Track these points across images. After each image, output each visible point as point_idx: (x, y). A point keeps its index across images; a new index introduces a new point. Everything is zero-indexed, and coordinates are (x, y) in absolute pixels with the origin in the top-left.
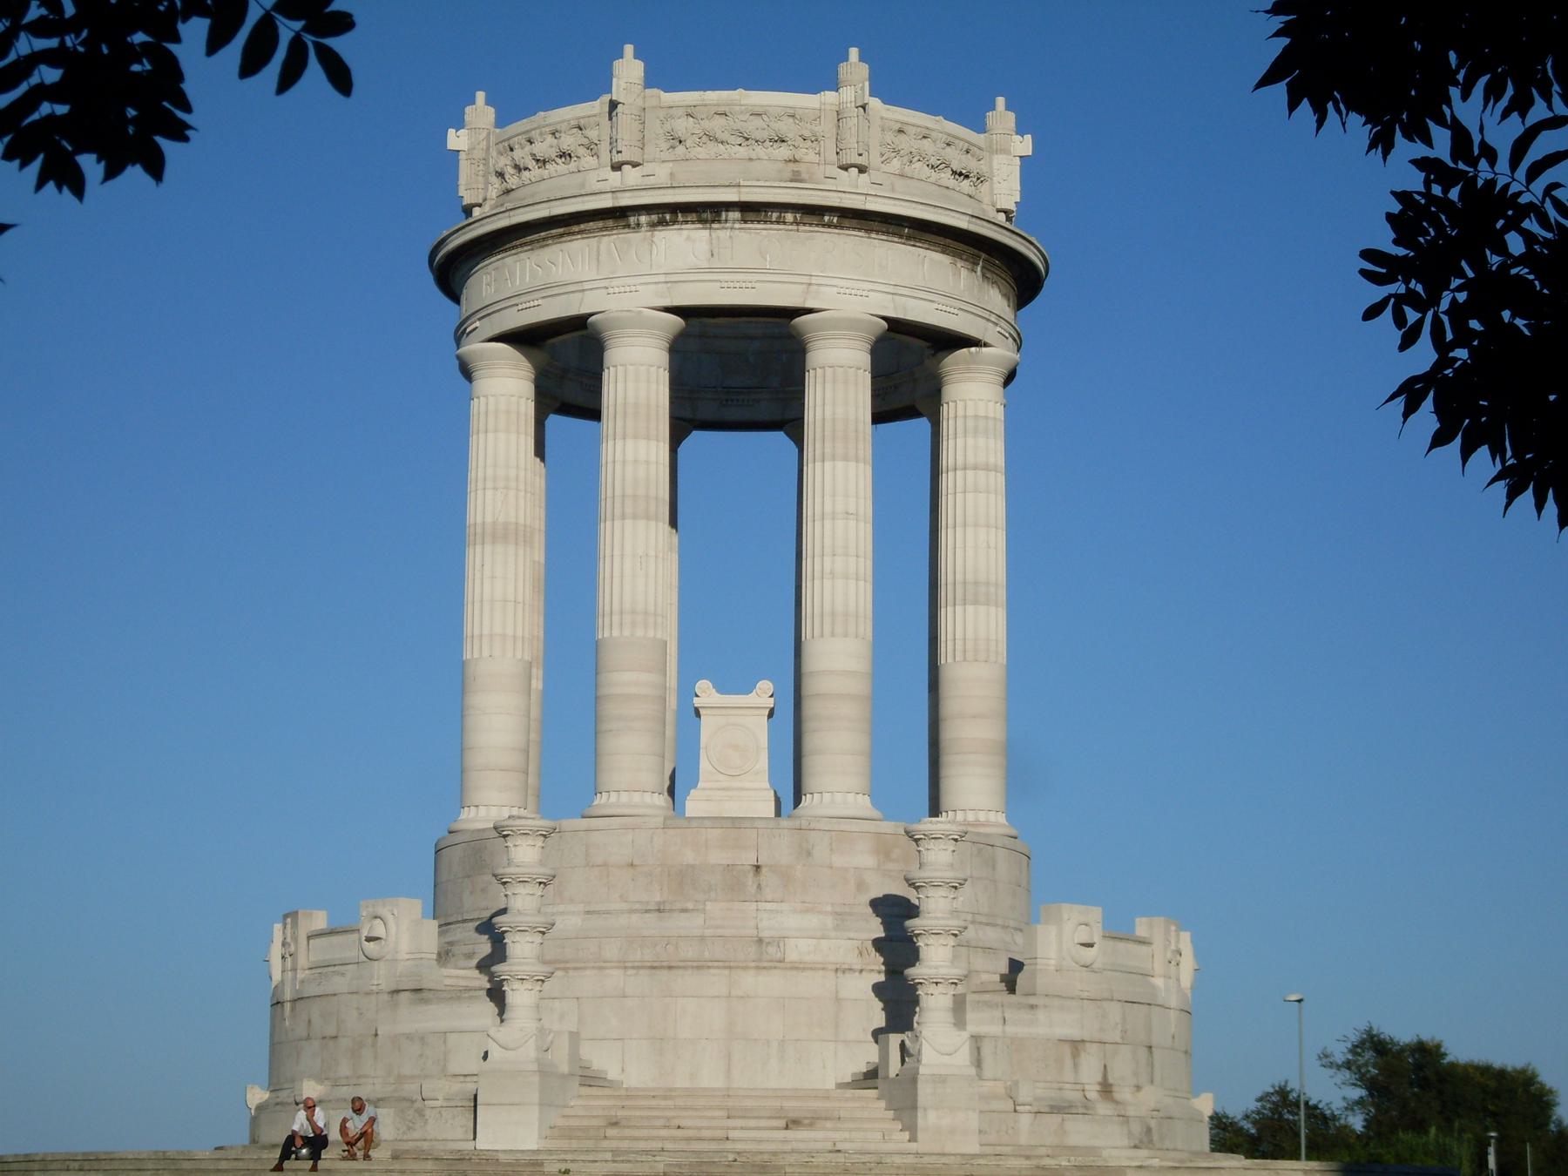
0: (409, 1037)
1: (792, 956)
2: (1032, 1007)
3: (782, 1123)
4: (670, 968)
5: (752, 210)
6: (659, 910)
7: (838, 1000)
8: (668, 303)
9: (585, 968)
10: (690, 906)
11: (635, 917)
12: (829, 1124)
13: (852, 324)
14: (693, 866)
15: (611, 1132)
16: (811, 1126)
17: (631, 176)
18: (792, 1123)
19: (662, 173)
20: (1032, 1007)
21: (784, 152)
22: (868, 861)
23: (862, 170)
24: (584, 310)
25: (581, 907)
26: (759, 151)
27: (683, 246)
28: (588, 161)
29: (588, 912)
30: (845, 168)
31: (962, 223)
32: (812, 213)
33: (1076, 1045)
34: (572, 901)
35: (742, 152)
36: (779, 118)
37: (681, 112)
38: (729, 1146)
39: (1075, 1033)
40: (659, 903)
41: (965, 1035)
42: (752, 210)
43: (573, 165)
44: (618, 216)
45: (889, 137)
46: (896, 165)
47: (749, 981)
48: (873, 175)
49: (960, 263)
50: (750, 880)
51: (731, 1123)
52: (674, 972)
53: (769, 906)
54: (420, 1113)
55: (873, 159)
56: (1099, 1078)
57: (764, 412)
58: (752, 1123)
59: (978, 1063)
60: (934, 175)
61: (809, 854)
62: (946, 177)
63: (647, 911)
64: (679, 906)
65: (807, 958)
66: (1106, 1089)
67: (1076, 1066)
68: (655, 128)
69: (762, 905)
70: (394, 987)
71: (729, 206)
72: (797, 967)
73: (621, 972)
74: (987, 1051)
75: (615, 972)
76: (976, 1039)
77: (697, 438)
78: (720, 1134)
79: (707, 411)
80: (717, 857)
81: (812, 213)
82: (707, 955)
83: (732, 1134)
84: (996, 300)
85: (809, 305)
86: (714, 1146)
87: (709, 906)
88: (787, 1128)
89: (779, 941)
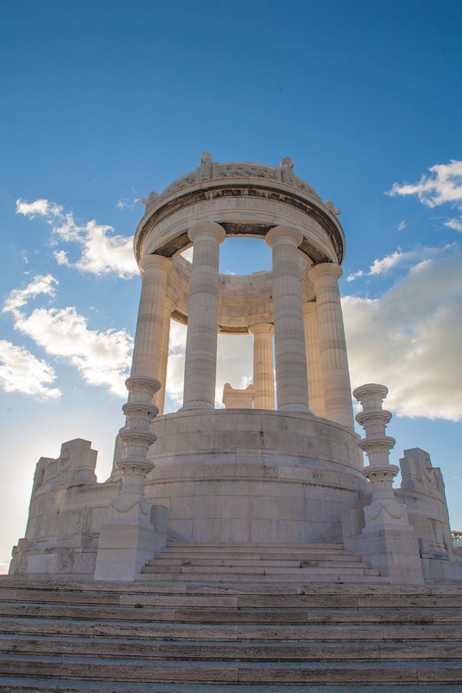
0: (73, 512)
1: (281, 476)
2: (415, 499)
3: (298, 564)
4: (218, 480)
6: (213, 453)
7: (305, 499)
8: (220, 220)
9: (174, 482)
10: (228, 450)
11: (200, 456)
12: (327, 565)
14: (230, 432)
15: (185, 569)
16: (316, 566)
18: (305, 564)
22: (313, 434)
25: (173, 454)
29: (177, 456)
34: (169, 451)
37: (225, 168)
38: (268, 579)
40: (212, 449)
50: (258, 438)
52: (221, 483)
53: (268, 451)
56: (443, 541)
58: (279, 564)
63: (207, 454)
64: (224, 451)
65: (288, 477)
69: (265, 451)
70: (70, 486)
72: (284, 481)
73: (192, 484)
75: (189, 484)
78: (260, 571)
80: (241, 427)
82: (238, 474)
85: (275, 223)
87: (238, 450)
88: (301, 567)
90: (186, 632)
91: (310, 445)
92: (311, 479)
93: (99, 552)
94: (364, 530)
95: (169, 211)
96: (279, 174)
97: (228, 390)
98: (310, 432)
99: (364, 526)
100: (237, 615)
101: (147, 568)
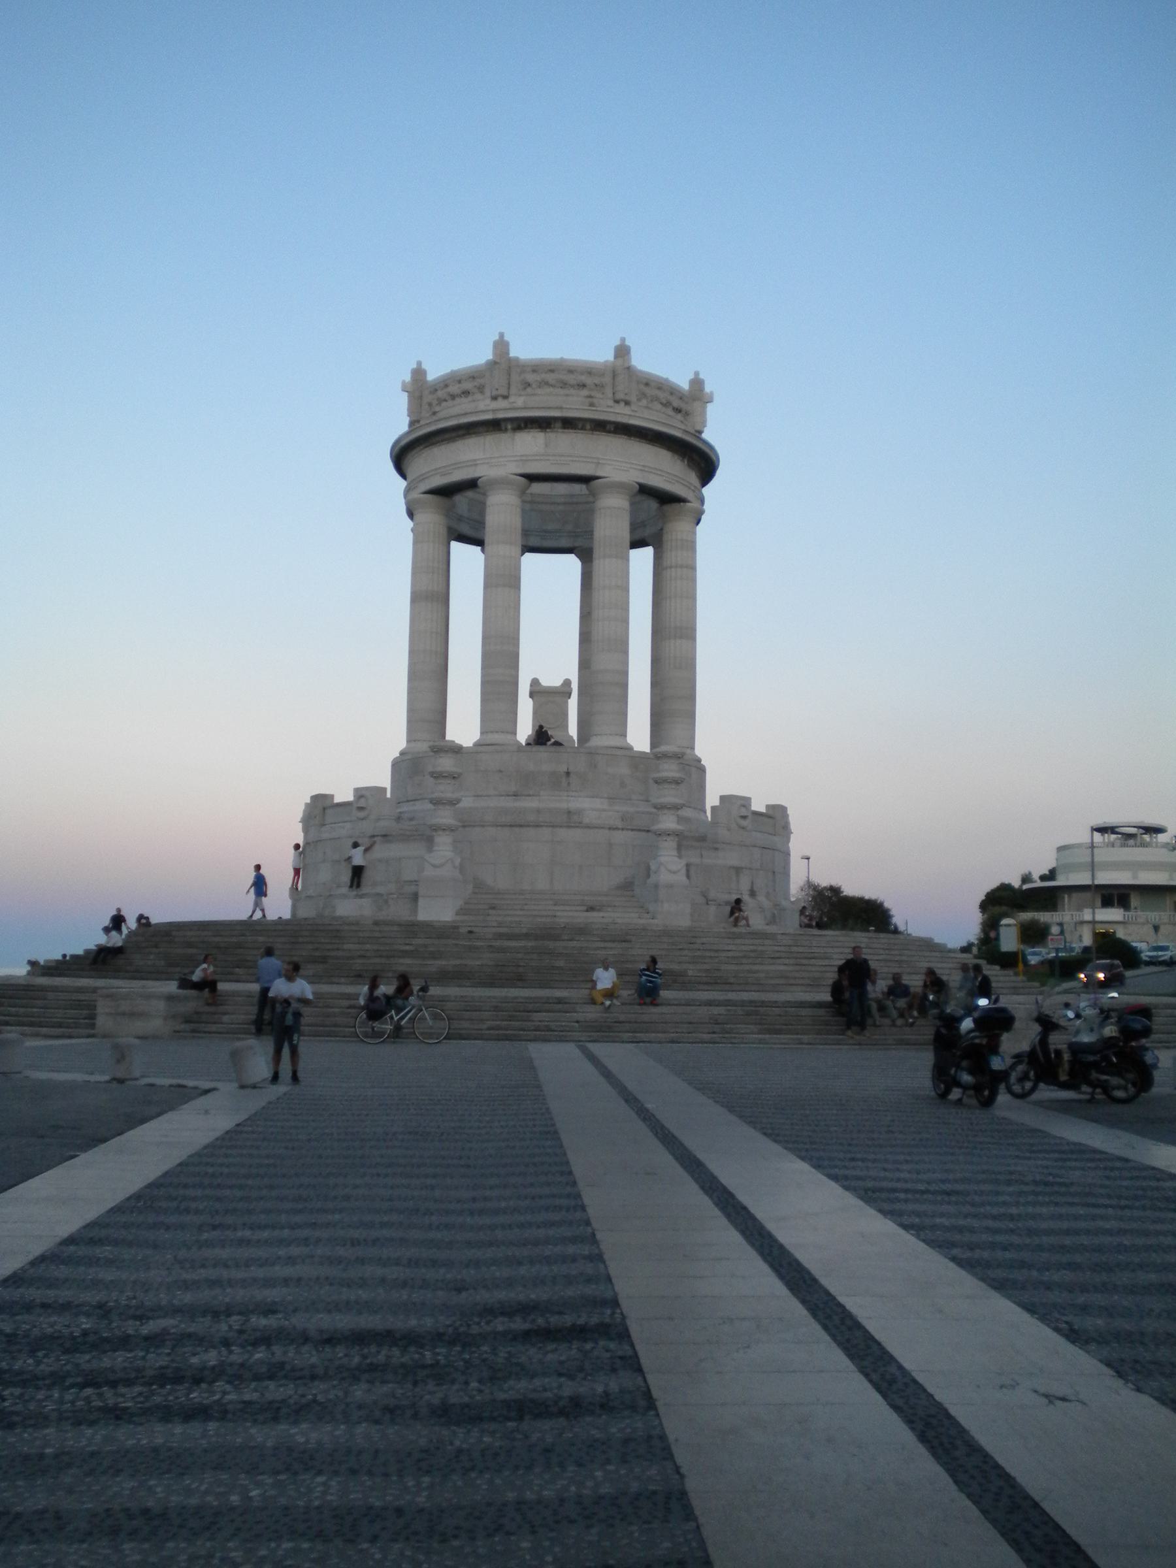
0: (380, 861)
1: (586, 821)
4: (521, 826)
5: (569, 424)
13: (620, 487)
15: (491, 912)
16: (599, 910)
17: (501, 403)
18: (591, 909)
19: (520, 402)
20: (716, 849)
21: (585, 392)
23: (627, 403)
24: (476, 475)
26: (572, 391)
27: (530, 443)
28: (478, 396)
30: (617, 402)
31: (678, 434)
32: (600, 426)
33: (738, 870)
35: (562, 392)
36: (582, 373)
39: (735, 863)
41: (684, 862)
42: (569, 424)
43: (470, 398)
44: (495, 425)
45: (642, 387)
46: (644, 402)
47: (563, 833)
48: (633, 407)
49: (676, 457)
50: (564, 779)
51: (556, 908)
54: (386, 902)
55: (633, 399)
57: (564, 543)
58: (567, 908)
59: (688, 876)
60: (664, 409)
61: (595, 766)
62: (670, 412)
66: (753, 894)
67: (738, 881)
68: (515, 378)
71: (555, 419)
72: (588, 827)
74: (692, 872)
76: (688, 865)
77: (528, 555)
79: (534, 541)
81: (600, 426)
83: (558, 914)
84: (693, 478)
85: (598, 474)
86: (548, 920)
89: (579, 812)
90: (498, 943)
91: (623, 785)
92: (620, 824)
93: (421, 902)
94: (649, 881)
95: (447, 436)
96: (607, 379)
97: (537, 689)
98: (624, 770)
99: (648, 876)
100: (527, 936)
101: (461, 912)
